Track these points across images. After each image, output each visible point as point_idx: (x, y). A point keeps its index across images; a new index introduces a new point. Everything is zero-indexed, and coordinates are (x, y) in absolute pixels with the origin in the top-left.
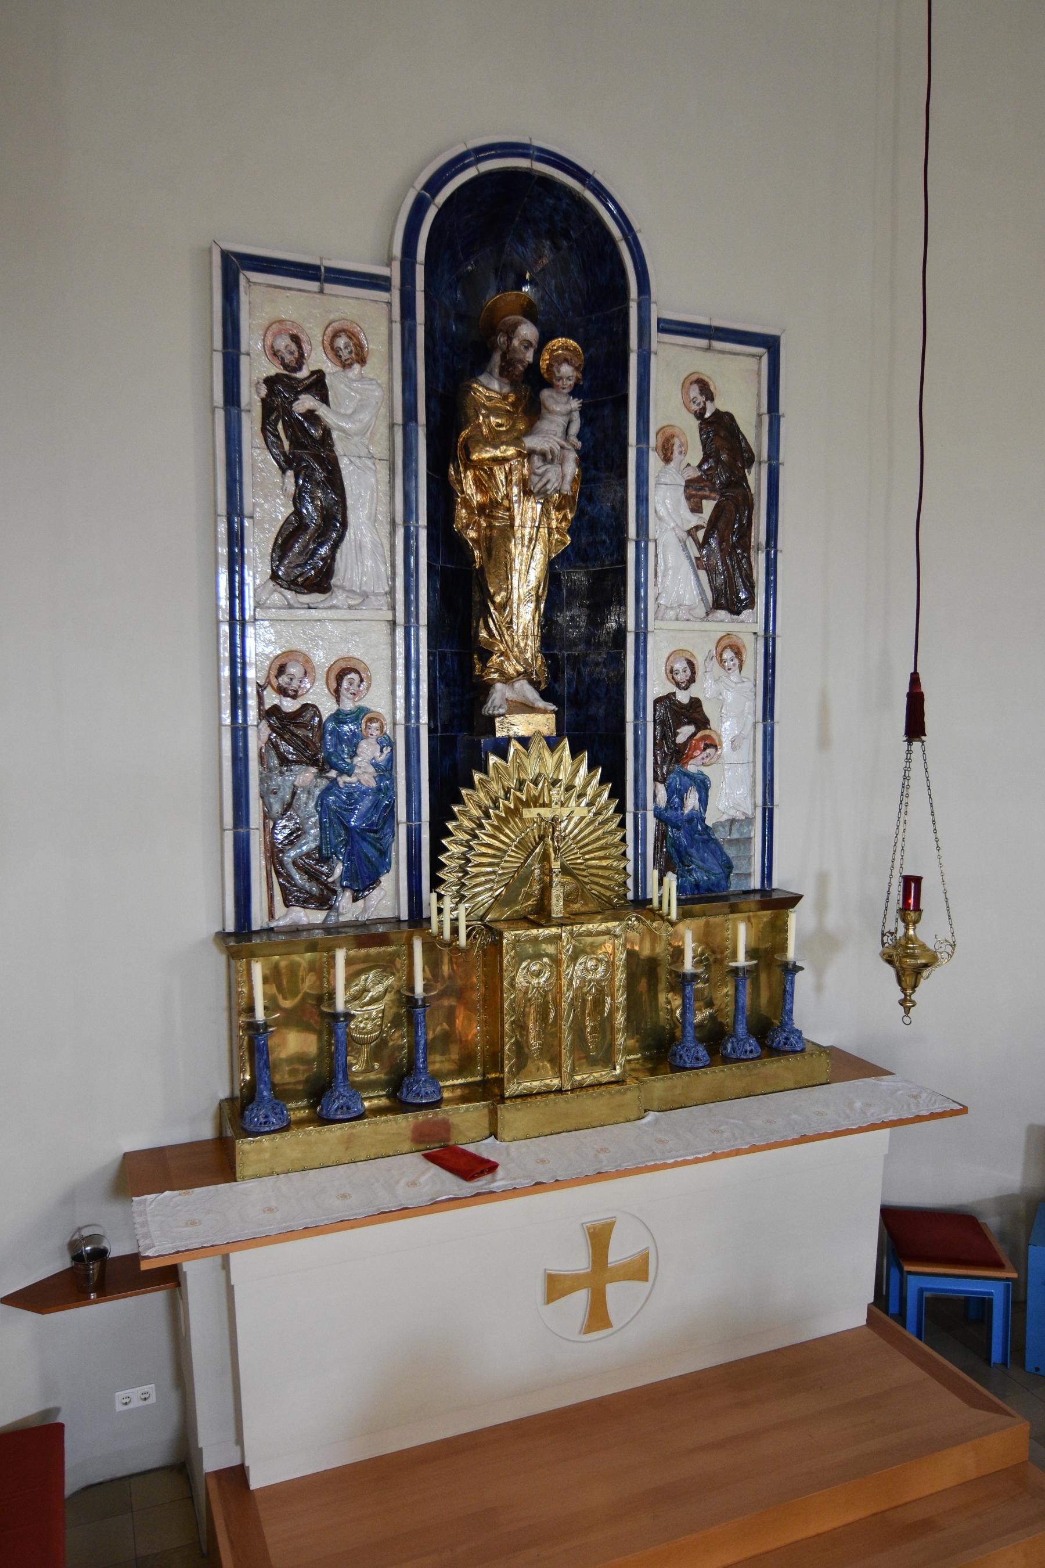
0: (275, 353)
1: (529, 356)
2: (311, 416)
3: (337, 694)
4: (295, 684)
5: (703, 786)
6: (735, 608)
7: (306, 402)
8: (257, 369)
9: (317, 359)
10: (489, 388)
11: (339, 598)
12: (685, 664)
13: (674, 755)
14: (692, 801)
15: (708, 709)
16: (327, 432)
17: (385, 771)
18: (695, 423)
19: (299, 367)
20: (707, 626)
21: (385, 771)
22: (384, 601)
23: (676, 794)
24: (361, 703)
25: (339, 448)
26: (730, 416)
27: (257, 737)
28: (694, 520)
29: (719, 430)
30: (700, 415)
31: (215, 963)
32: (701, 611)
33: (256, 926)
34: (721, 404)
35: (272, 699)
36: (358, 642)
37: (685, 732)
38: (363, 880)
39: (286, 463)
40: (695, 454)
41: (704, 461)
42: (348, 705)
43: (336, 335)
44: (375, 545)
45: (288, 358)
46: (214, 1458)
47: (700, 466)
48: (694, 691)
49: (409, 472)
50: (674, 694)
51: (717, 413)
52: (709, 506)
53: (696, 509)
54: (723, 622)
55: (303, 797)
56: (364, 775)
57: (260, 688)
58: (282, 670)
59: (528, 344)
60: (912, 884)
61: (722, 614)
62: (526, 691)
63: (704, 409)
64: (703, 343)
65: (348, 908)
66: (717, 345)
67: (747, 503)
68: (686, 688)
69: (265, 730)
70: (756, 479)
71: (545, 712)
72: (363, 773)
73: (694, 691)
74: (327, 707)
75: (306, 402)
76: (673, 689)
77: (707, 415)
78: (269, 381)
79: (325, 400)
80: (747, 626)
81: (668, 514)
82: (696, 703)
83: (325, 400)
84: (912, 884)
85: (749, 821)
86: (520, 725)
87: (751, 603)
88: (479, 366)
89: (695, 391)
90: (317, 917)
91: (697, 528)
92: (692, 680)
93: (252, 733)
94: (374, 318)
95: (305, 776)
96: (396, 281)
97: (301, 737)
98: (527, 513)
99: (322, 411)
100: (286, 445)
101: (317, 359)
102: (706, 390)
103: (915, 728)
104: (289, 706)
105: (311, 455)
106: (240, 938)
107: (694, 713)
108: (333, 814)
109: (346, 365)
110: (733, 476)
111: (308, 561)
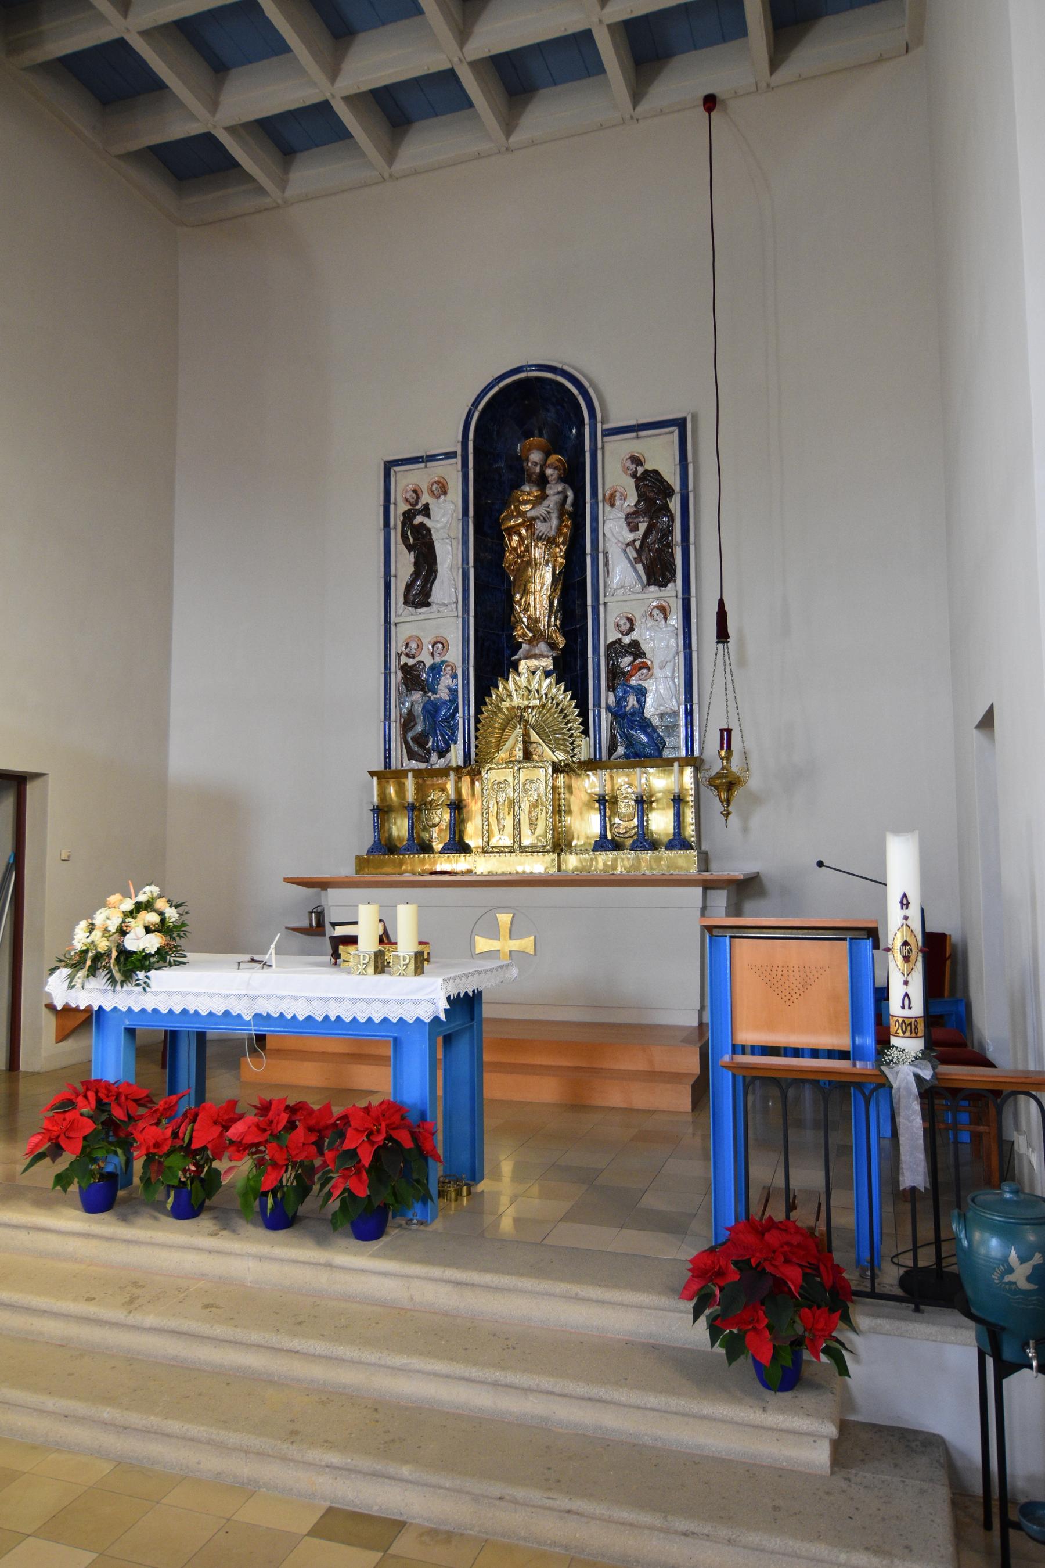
0: (407, 500)
1: (538, 469)
2: (422, 524)
3: (432, 655)
4: (413, 651)
5: (641, 693)
6: (663, 584)
9: (426, 498)
11: (434, 608)
12: (625, 620)
14: (632, 701)
15: (644, 647)
16: (429, 531)
17: (453, 692)
18: (632, 481)
19: (417, 503)
20: (641, 596)
21: (453, 692)
22: (454, 606)
24: (445, 658)
25: (434, 537)
26: (656, 472)
27: (397, 677)
28: (631, 537)
30: (634, 475)
32: (638, 587)
33: (393, 768)
34: (649, 466)
35: (404, 660)
36: (443, 629)
37: (625, 661)
39: (410, 548)
40: (633, 499)
41: (638, 502)
42: (438, 659)
43: (432, 485)
45: (412, 500)
47: (635, 505)
48: (635, 635)
50: (620, 640)
51: (646, 472)
52: (643, 527)
53: (634, 528)
55: (416, 706)
56: (443, 694)
57: (399, 655)
58: (407, 645)
59: (536, 464)
61: (652, 588)
62: (542, 647)
63: (636, 471)
64: (634, 435)
65: (438, 763)
66: (642, 434)
68: (627, 634)
69: (400, 674)
70: (675, 505)
71: (548, 657)
73: (635, 635)
75: (419, 519)
76: (620, 636)
77: (639, 474)
79: (428, 515)
82: (635, 644)
83: (428, 515)
85: (676, 714)
89: (629, 463)
90: (422, 766)
91: (634, 541)
92: (632, 629)
93: (393, 676)
94: (451, 472)
95: (417, 696)
96: (459, 453)
97: (412, 678)
98: (538, 553)
99: (427, 522)
100: (411, 540)
104: (411, 662)
106: (386, 774)
107: (635, 650)
109: (438, 497)
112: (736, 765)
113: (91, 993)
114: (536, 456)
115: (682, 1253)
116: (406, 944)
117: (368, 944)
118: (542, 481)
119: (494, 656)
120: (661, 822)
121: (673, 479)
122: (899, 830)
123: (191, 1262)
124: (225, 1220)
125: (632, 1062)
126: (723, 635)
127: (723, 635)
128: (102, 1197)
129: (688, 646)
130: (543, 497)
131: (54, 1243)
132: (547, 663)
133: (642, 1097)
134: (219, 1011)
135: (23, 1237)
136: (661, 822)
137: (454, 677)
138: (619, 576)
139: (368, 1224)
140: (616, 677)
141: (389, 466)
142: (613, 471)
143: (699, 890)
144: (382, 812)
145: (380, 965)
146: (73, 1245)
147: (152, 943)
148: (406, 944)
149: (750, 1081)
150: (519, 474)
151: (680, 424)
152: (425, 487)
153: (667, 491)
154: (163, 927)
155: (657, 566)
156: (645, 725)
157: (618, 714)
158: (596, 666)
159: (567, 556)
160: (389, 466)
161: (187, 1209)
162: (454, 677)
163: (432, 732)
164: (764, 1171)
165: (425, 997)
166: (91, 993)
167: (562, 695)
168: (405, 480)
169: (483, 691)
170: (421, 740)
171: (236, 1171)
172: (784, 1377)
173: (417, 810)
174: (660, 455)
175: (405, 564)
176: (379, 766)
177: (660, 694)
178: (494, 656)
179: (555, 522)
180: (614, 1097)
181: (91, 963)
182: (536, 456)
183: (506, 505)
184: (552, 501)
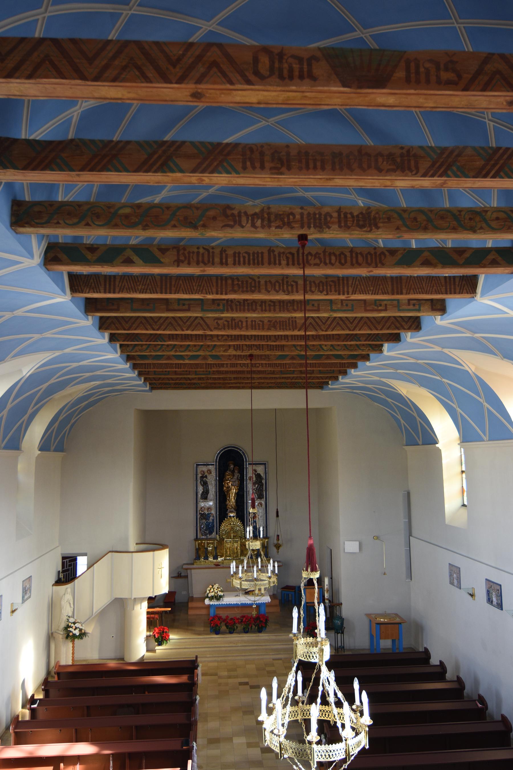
7: (205, 479)
8: (200, 475)
9: (206, 474)
10: (228, 473)
17: (213, 520)
18: (254, 476)
21: (213, 520)
28: (254, 488)
31: (194, 542)
34: (258, 472)
35: (200, 512)
38: (211, 533)
39: (203, 486)
40: (254, 479)
46: (190, 596)
49: (216, 486)
52: (257, 485)
56: (211, 521)
60: (278, 536)
62: (233, 510)
65: (209, 536)
67: (263, 485)
70: (264, 481)
72: (211, 521)
74: (207, 513)
78: (201, 477)
81: (250, 488)
84: (278, 536)
87: (263, 498)
88: (226, 471)
95: (204, 521)
101: (206, 474)
102: (255, 471)
103: (277, 516)
104: (202, 513)
105: (205, 484)
106: (196, 539)
108: (207, 525)
110: (260, 482)
112: (280, 542)
113: (214, 602)
114: (232, 466)
118: (233, 472)
121: (263, 475)
122: (326, 576)
123: (237, 639)
128: (217, 633)
129: (266, 513)
130: (233, 476)
131: (213, 639)
134: (235, 603)
135: (208, 640)
137: (213, 517)
139: (260, 631)
142: (249, 472)
145: (258, 595)
146: (217, 639)
147: (222, 594)
151: (265, 464)
154: (221, 591)
162: (213, 517)
166: (214, 602)
174: (260, 470)
175: (201, 489)
179: (237, 482)
184: (236, 477)
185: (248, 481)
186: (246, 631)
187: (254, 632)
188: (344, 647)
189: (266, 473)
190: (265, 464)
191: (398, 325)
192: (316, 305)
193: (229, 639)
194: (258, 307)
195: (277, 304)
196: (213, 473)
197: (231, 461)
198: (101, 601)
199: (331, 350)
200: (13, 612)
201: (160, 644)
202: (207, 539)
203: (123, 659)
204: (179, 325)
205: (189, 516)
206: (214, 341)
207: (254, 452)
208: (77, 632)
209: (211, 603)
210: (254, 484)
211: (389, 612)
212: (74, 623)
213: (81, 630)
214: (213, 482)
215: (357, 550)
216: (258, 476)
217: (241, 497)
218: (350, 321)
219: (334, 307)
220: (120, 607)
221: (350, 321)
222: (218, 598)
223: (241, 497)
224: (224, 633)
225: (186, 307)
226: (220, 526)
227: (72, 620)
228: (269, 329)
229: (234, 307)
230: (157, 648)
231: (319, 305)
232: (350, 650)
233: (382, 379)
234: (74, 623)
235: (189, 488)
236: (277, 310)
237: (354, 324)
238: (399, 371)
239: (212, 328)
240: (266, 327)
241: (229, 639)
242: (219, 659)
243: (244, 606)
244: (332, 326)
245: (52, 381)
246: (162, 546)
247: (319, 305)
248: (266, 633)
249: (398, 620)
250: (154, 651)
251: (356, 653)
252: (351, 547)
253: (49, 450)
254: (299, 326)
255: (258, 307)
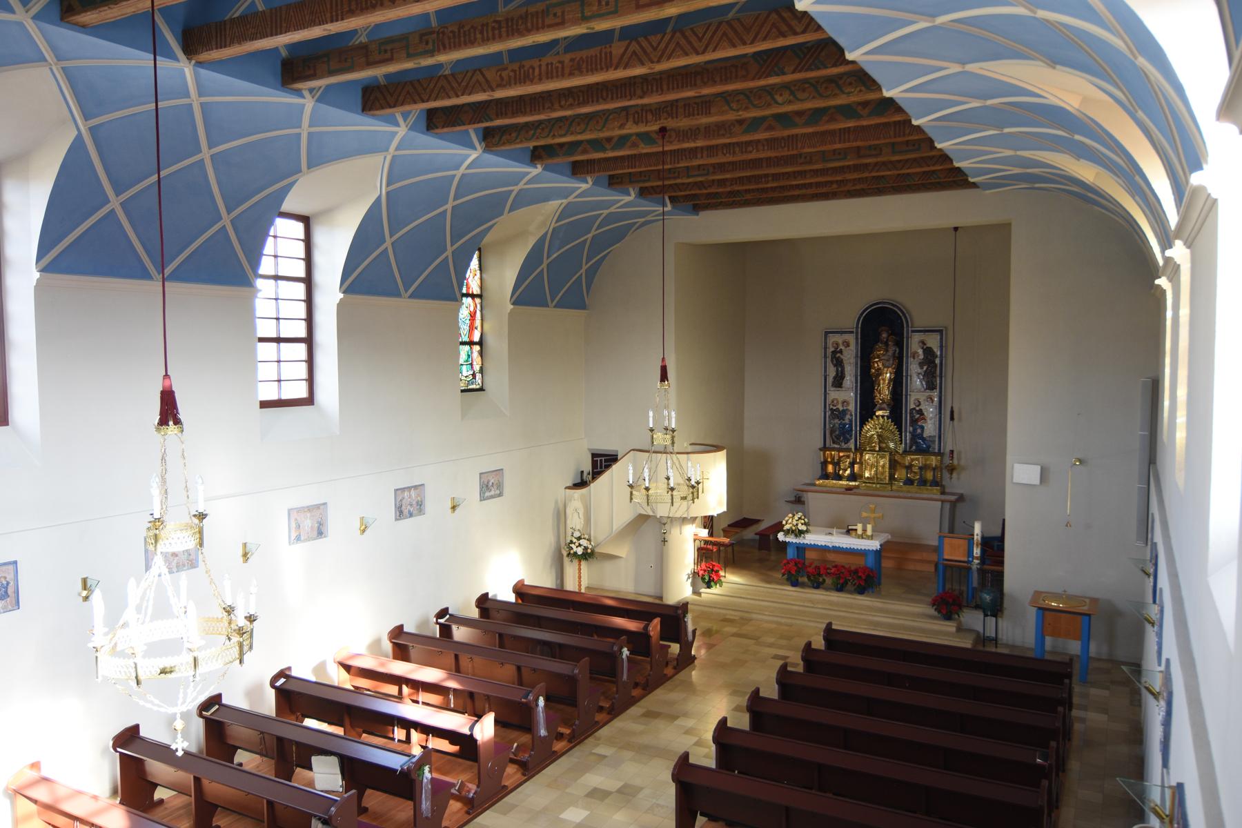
5: (922, 428)
13: (914, 422)
23: (915, 430)
29: (928, 352)
36: (848, 396)
38: (847, 441)
39: (835, 365)
44: (849, 380)
54: (928, 393)
60: (952, 452)
65: (845, 446)
70: (937, 361)
80: (935, 394)
86: (879, 413)
94: (851, 339)
102: (923, 343)
105: (839, 363)
106: (824, 449)
107: (920, 412)
110: (930, 363)
111: (838, 382)
112: (955, 462)
113: (791, 539)
115: (930, 600)
116: (869, 532)
117: (860, 532)
118: (886, 344)
119: (867, 411)
120: (929, 475)
124: (827, 589)
125: (917, 556)
126: (952, 418)
127: (952, 418)
128: (795, 584)
132: (887, 413)
133: (919, 567)
136: (929, 475)
138: (916, 382)
139: (861, 591)
140: (914, 422)
141: (827, 333)
142: (914, 344)
143: (939, 503)
144: (824, 464)
145: (861, 537)
147: (804, 528)
148: (869, 532)
149: (946, 567)
150: (877, 340)
151: (940, 332)
152: (840, 342)
153: (934, 355)
154: (805, 524)
155: (931, 386)
156: (924, 439)
157: (914, 437)
158: (906, 419)
159: (896, 373)
160: (827, 333)
161: (817, 587)
163: (839, 432)
164: (948, 586)
165: (874, 545)
167: (893, 427)
168: (833, 339)
169: (863, 423)
170: (838, 437)
171: (829, 581)
172: (948, 617)
173: (837, 464)
174: (933, 342)
175: (832, 372)
176: (821, 445)
177: (930, 429)
178: (867, 411)
180: (911, 567)
181: (787, 532)
182: (884, 335)
183: (872, 352)
184: (890, 353)
185: (911, 360)
186: (840, 588)
187: (851, 592)
188: (996, 639)
189: (941, 347)
190: (940, 332)
191: (784, 28)
192: (559, 14)
193: (809, 596)
194: (479, 36)
195: (503, 24)
196: (853, 346)
197: (882, 326)
198: (623, 516)
199: (790, 102)
200: (454, 508)
201: (709, 587)
202: (839, 450)
203: (661, 598)
204: (453, 88)
205: (814, 414)
206: (555, 110)
207: (922, 309)
208: (580, 551)
209: (787, 540)
210: (921, 365)
211: (1073, 591)
212: (579, 538)
213: (586, 548)
214: (853, 360)
215: (1036, 481)
216: (928, 352)
217: (898, 384)
218: (697, 35)
219: (587, 13)
220: (649, 528)
221: (697, 35)
222: (800, 533)
223: (898, 384)
224: (803, 585)
225: (388, 55)
226: (861, 427)
227: (577, 534)
228: (571, 74)
229: (447, 42)
230: (703, 590)
231: (563, 13)
232: (1007, 646)
233: (1019, 153)
234: (579, 538)
235: (815, 370)
236: (504, 34)
237: (705, 41)
238: (1006, 130)
239: (494, 85)
240: (567, 71)
241: (809, 596)
242: (783, 621)
243: (837, 550)
244: (668, 51)
245: (612, 209)
246: (717, 448)
247: (563, 13)
248: (878, 595)
249: (1085, 609)
250: (699, 594)
251: (1016, 653)
252: (1023, 473)
253: (540, 302)
254: (615, 61)
255: (479, 36)
